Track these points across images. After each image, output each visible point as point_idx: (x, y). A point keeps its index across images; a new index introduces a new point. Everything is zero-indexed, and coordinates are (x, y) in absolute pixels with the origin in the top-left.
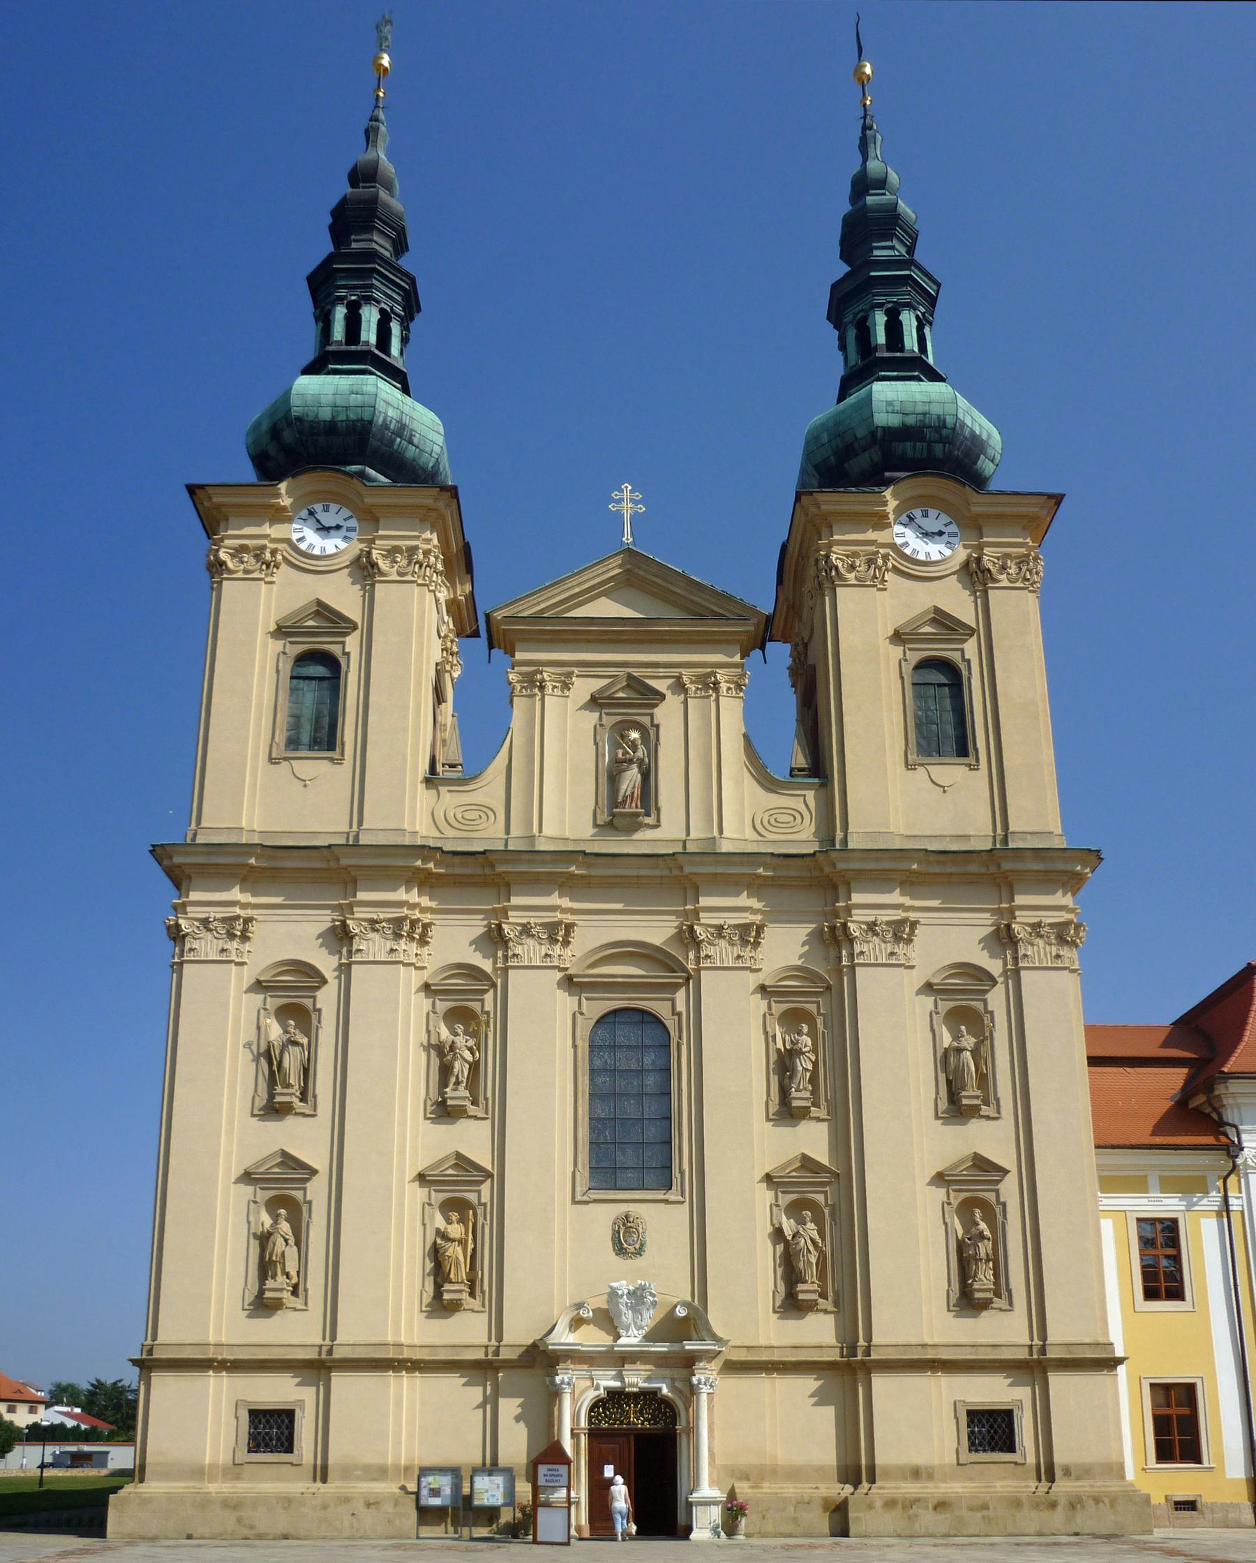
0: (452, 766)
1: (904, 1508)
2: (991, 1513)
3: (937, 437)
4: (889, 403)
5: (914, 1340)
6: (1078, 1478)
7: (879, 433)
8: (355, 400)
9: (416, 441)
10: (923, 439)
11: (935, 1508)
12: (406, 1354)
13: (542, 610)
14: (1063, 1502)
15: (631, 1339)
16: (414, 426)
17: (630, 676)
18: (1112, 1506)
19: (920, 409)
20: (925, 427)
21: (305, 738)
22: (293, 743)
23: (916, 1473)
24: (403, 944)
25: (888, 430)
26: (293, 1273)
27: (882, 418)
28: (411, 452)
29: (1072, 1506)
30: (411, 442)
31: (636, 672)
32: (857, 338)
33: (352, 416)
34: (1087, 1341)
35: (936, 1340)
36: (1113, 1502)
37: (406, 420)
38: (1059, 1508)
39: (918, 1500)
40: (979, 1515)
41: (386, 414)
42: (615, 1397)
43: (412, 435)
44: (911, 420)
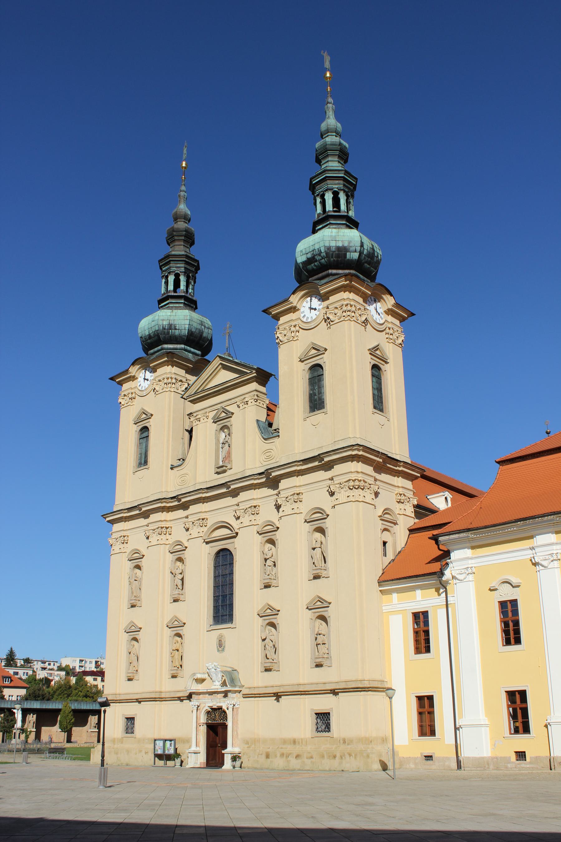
0: (180, 460)
1: (286, 757)
2: (313, 760)
3: (320, 258)
4: (301, 251)
5: (296, 682)
6: (348, 744)
7: (301, 265)
8: (153, 324)
9: (177, 328)
10: (316, 261)
11: (296, 758)
12: (163, 695)
13: (198, 389)
14: (338, 756)
15: (217, 686)
16: (176, 322)
17: (223, 408)
18: (355, 758)
19: (311, 249)
20: (315, 256)
21: (143, 462)
22: (140, 464)
23: (294, 742)
24: (163, 536)
25: (303, 263)
26: (136, 666)
27: (301, 259)
28: (177, 333)
29: (341, 757)
30: (176, 329)
31: (223, 405)
32: (175, 280)
33: (153, 331)
34: (354, 679)
35: (306, 682)
36: (356, 755)
37: (172, 322)
38: (337, 758)
39: (290, 754)
40: (310, 760)
41: (163, 325)
42: (214, 710)
43: (175, 327)
44: (309, 256)
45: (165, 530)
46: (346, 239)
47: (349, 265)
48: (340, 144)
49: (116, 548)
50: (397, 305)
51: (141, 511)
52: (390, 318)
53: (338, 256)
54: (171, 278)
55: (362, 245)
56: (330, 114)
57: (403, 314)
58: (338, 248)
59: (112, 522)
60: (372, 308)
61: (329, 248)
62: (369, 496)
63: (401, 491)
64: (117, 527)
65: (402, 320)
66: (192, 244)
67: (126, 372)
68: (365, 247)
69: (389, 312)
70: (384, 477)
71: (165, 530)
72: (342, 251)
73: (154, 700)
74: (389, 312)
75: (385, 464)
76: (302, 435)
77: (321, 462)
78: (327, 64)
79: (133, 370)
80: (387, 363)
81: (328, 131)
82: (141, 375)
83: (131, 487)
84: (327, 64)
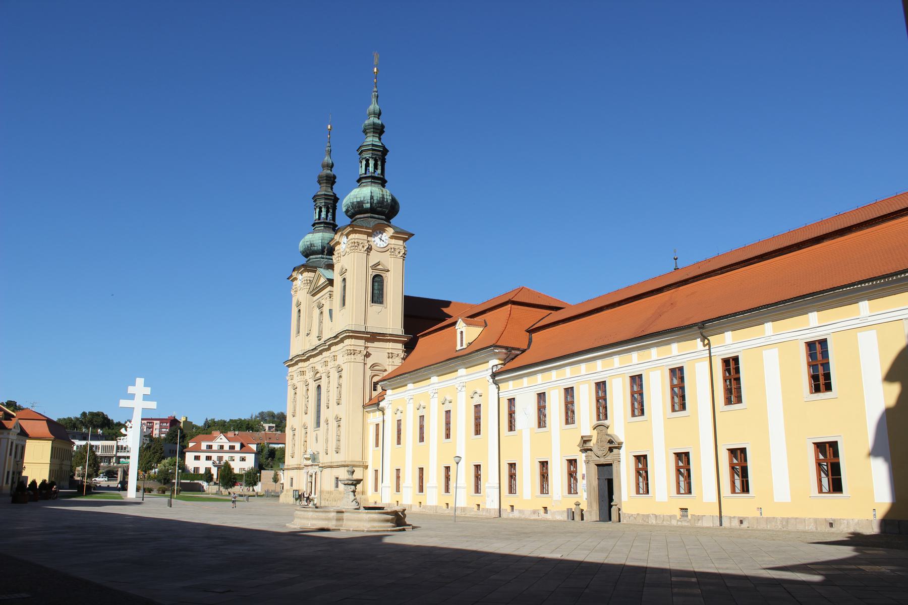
45: (303, 373)
46: (362, 196)
47: (366, 211)
48: (374, 124)
49: (290, 381)
50: (396, 232)
51: (306, 357)
52: (393, 241)
53: (359, 207)
54: (318, 210)
55: (372, 197)
56: (374, 100)
57: (404, 235)
58: (358, 202)
59: (289, 366)
60: (377, 239)
61: (353, 203)
62: (360, 358)
63: (390, 351)
64: (290, 369)
65: (405, 240)
66: (333, 183)
67: (291, 276)
68: (375, 198)
69: (392, 237)
70: (376, 344)
71: (303, 373)
72: (360, 204)
73: (297, 469)
74: (392, 237)
75: (374, 337)
76: (345, 320)
77: (338, 339)
78: (376, 61)
79: (295, 274)
80: (388, 271)
81: (370, 114)
82: (300, 277)
83: (298, 346)
84: (376, 61)
